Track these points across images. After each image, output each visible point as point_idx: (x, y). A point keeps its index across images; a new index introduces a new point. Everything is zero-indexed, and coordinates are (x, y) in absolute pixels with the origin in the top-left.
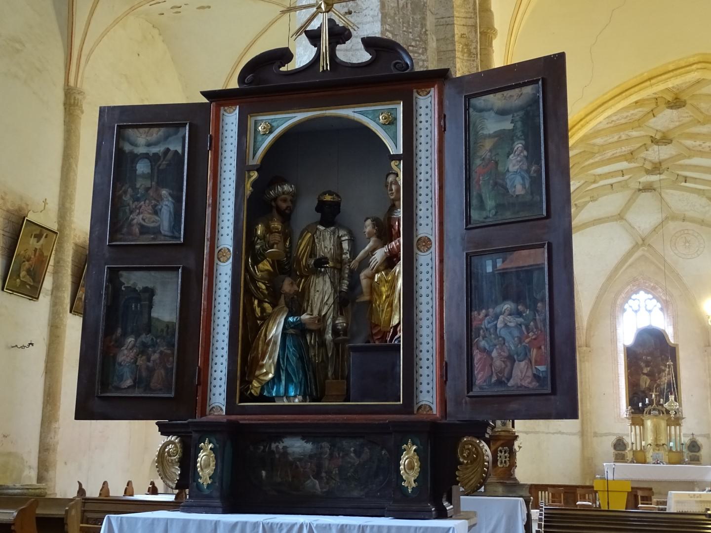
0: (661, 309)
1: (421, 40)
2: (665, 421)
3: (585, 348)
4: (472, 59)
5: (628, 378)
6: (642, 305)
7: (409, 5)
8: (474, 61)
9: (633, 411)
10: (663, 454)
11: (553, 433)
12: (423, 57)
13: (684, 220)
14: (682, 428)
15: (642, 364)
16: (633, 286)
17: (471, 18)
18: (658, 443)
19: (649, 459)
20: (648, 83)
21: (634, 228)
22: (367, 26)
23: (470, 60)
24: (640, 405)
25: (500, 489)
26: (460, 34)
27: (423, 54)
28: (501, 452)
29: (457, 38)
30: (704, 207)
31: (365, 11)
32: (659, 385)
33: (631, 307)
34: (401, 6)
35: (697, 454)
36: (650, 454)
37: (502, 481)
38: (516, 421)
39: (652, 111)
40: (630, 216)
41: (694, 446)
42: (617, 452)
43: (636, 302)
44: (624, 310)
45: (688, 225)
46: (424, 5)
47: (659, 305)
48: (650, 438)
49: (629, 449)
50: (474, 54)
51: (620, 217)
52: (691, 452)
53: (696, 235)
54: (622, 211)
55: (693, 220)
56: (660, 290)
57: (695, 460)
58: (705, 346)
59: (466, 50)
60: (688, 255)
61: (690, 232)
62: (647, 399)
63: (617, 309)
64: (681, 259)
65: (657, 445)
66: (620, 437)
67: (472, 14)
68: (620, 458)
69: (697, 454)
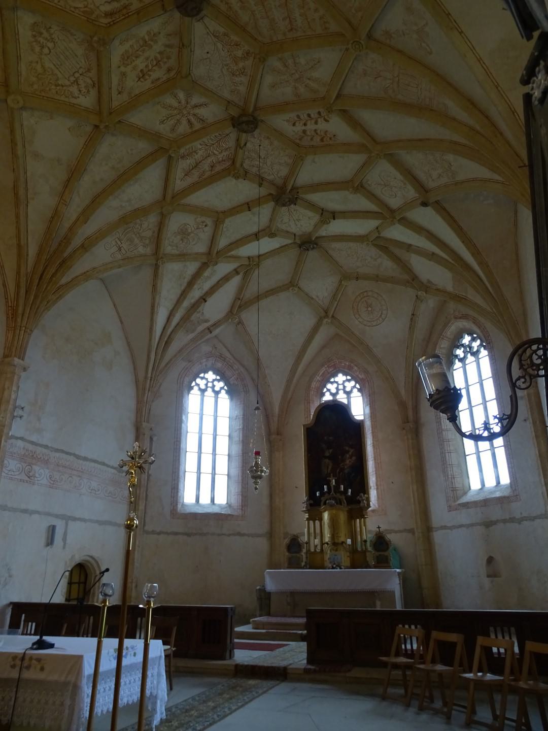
0: (359, 390)
2: (346, 513)
5: (308, 462)
6: (341, 387)
9: (312, 502)
11: (229, 535)
13: (357, 279)
14: (367, 520)
16: (329, 367)
18: (336, 541)
19: (327, 564)
21: (312, 298)
24: (318, 494)
35: (386, 554)
36: (328, 554)
39: (377, 228)
43: (335, 385)
47: (358, 386)
48: (327, 537)
49: (304, 550)
51: (292, 284)
55: (366, 277)
56: (356, 368)
57: (383, 562)
60: (373, 321)
61: (370, 294)
63: (312, 393)
64: (367, 328)
66: (294, 535)
68: (293, 563)
69: (386, 554)
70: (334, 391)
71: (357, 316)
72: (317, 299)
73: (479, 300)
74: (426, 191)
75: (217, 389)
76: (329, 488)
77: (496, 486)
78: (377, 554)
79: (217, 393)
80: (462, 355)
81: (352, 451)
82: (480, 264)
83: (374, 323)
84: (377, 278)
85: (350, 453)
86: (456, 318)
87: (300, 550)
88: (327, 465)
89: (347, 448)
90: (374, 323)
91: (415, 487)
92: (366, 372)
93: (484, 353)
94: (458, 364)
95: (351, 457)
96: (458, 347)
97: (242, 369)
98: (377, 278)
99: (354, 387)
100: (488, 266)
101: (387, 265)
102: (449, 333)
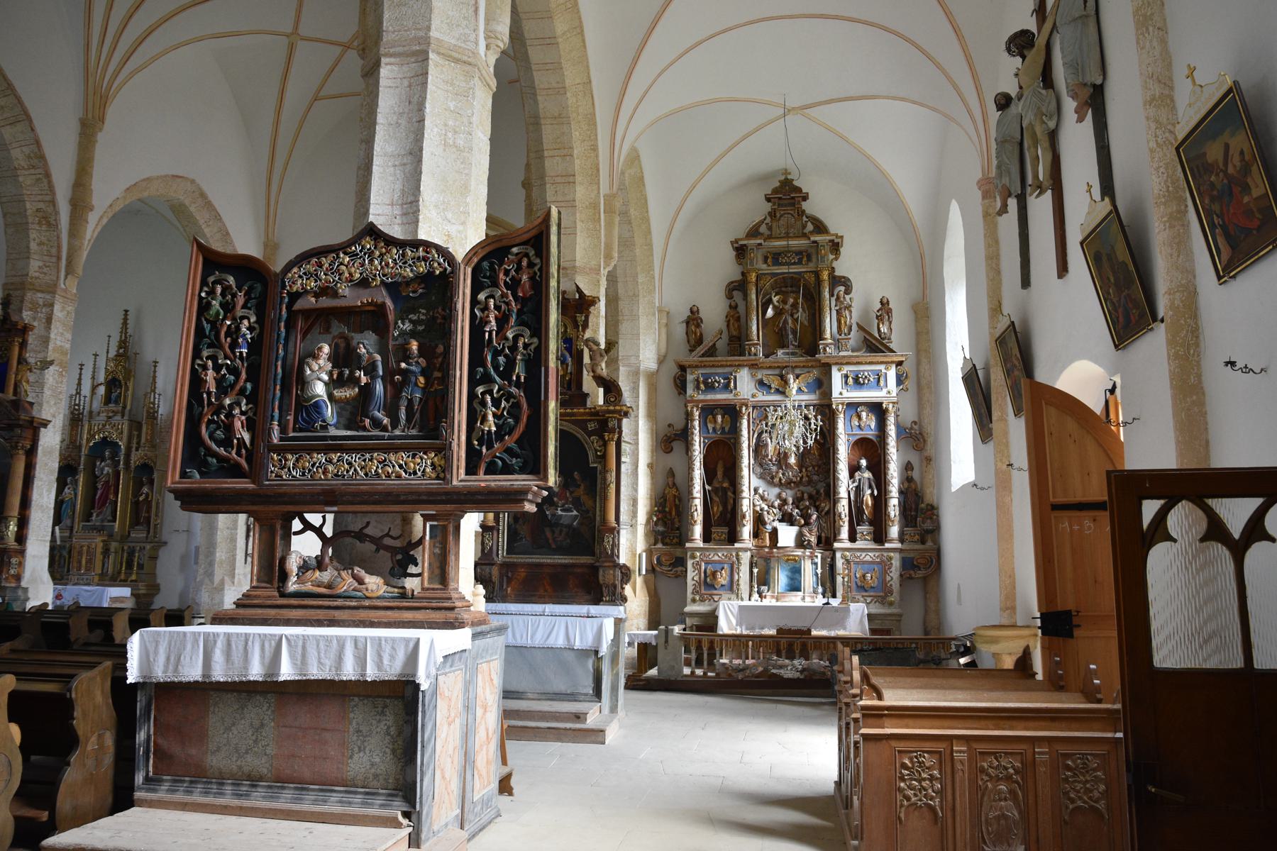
17: (47, 194)
26: (34, 209)
29: (29, 212)
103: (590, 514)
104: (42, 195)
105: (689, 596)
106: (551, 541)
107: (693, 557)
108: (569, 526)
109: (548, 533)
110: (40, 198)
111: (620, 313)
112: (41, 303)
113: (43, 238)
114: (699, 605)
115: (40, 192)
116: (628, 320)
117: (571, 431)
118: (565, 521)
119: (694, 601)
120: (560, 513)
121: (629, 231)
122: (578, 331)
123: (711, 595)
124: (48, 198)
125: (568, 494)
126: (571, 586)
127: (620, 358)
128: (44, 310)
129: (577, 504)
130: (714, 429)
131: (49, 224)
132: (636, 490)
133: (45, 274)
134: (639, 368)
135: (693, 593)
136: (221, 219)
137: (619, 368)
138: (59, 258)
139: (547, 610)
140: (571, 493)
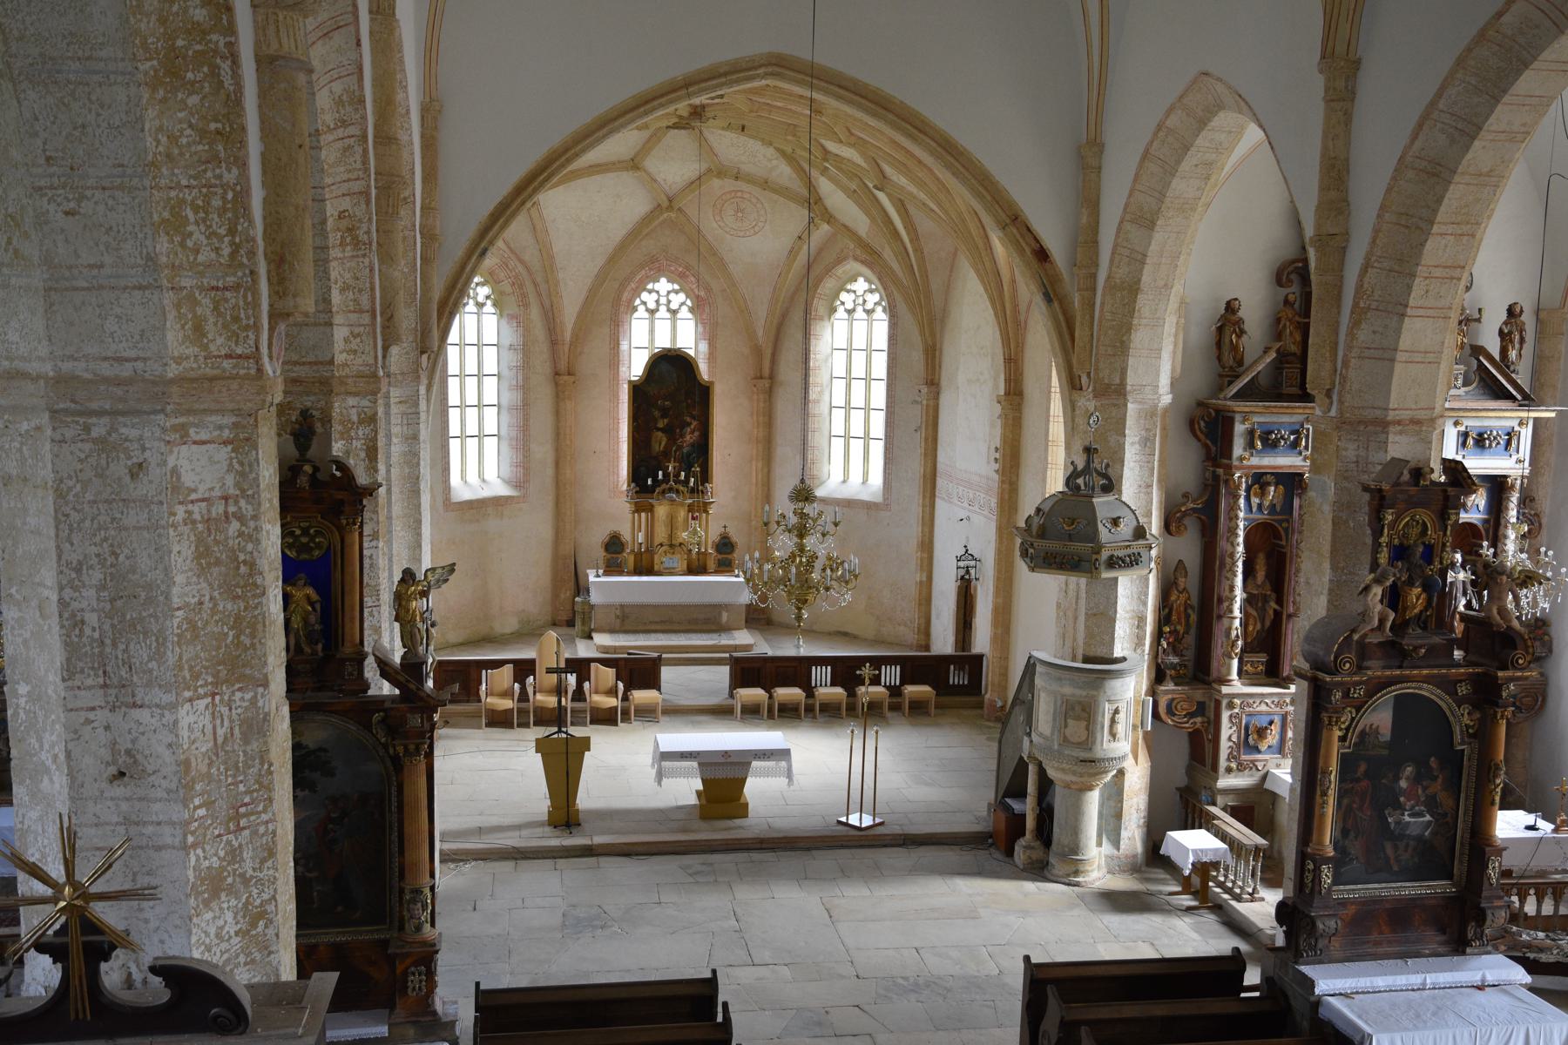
0: (691, 310)
1: (261, 784)
3: (566, 378)
4: (360, 253)
5: (633, 436)
6: (663, 300)
7: (237, 731)
8: (364, 256)
10: (679, 561)
12: (264, 817)
15: (657, 413)
16: (650, 269)
18: (674, 542)
20: (684, 92)
21: (655, 181)
22: (157, 807)
23: (357, 256)
24: (650, 482)
25: (411, 1032)
26: (336, 214)
27: (265, 811)
28: (414, 974)
30: (770, 160)
31: (153, 778)
32: (680, 448)
33: (644, 303)
34: (220, 740)
35: (729, 557)
37: (414, 1019)
38: (449, 373)
40: (652, 164)
41: (725, 545)
42: (609, 556)
43: (654, 296)
44: (635, 309)
45: (741, 185)
46: (265, 719)
47: (689, 303)
48: (661, 534)
50: (365, 244)
51: (633, 164)
52: (720, 553)
53: (754, 200)
54: (636, 155)
56: (693, 279)
57: (725, 566)
58: (756, 378)
59: (348, 240)
61: (746, 196)
62: (660, 473)
63: (622, 309)
64: (728, 236)
65: (671, 546)
67: (360, 173)
68: (612, 568)
69: (729, 557)
70: (652, 305)
71: (718, 218)
72: (662, 183)
73: (895, 266)
74: (885, 177)
75: (481, 299)
76: (666, 475)
77: (863, 483)
78: (720, 557)
79: (480, 305)
80: (850, 306)
81: (695, 423)
82: (915, 250)
83: (742, 234)
84: (765, 184)
85: (692, 427)
86: (856, 259)
87: (622, 550)
88: (659, 441)
89: (688, 419)
90: (742, 234)
91: (760, 465)
92: (708, 289)
93: (880, 314)
94: (841, 313)
95: (692, 432)
96: (848, 291)
97: (520, 268)
98: (765, 184)
99: (683, 304)
100: (922, 253)
101: (783, 173)
102: (840, 271)
103: (1449, 819)
104: (349, 180)
105: (1223, 763)
106: (1392, 861)
107: (1231, 706)
108: (1420, 839)
109: (1389, 851)
110: (345, 188)
111: (1136, 314)
112: (355, 418)
113: (347, 276)
114: (1236, 777)
115: (345, 177)
116: (1146, 325)
117: (1433, 697)
118: (1413, 831)
119: (1229, 770)
120: (1407, 819)
121: (1198, 189)
122: (1445, 534)
123: (1253, 762)
124: (357, 186)
125: (1420, 791)
126: (1417, 924)
127: (1129, 388)
128: (360, 433)
129: (1432, 804)
130: (1260, 506)
131: (356, 243)
132: (1145, 604)
133: (355, 352)
134: (1156, 406)
135: (1228, 760)
136: (406, 87)
137: (1126, 405)
138: (374, 316)
139: (1428, 981)
140: (1425, 789)
